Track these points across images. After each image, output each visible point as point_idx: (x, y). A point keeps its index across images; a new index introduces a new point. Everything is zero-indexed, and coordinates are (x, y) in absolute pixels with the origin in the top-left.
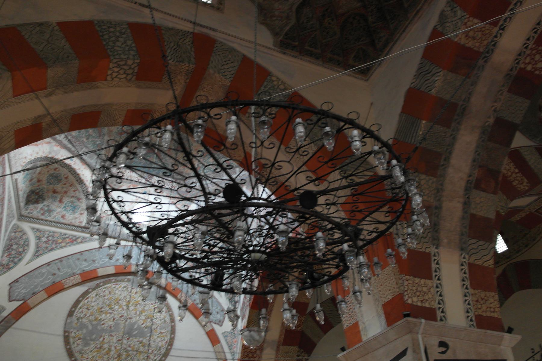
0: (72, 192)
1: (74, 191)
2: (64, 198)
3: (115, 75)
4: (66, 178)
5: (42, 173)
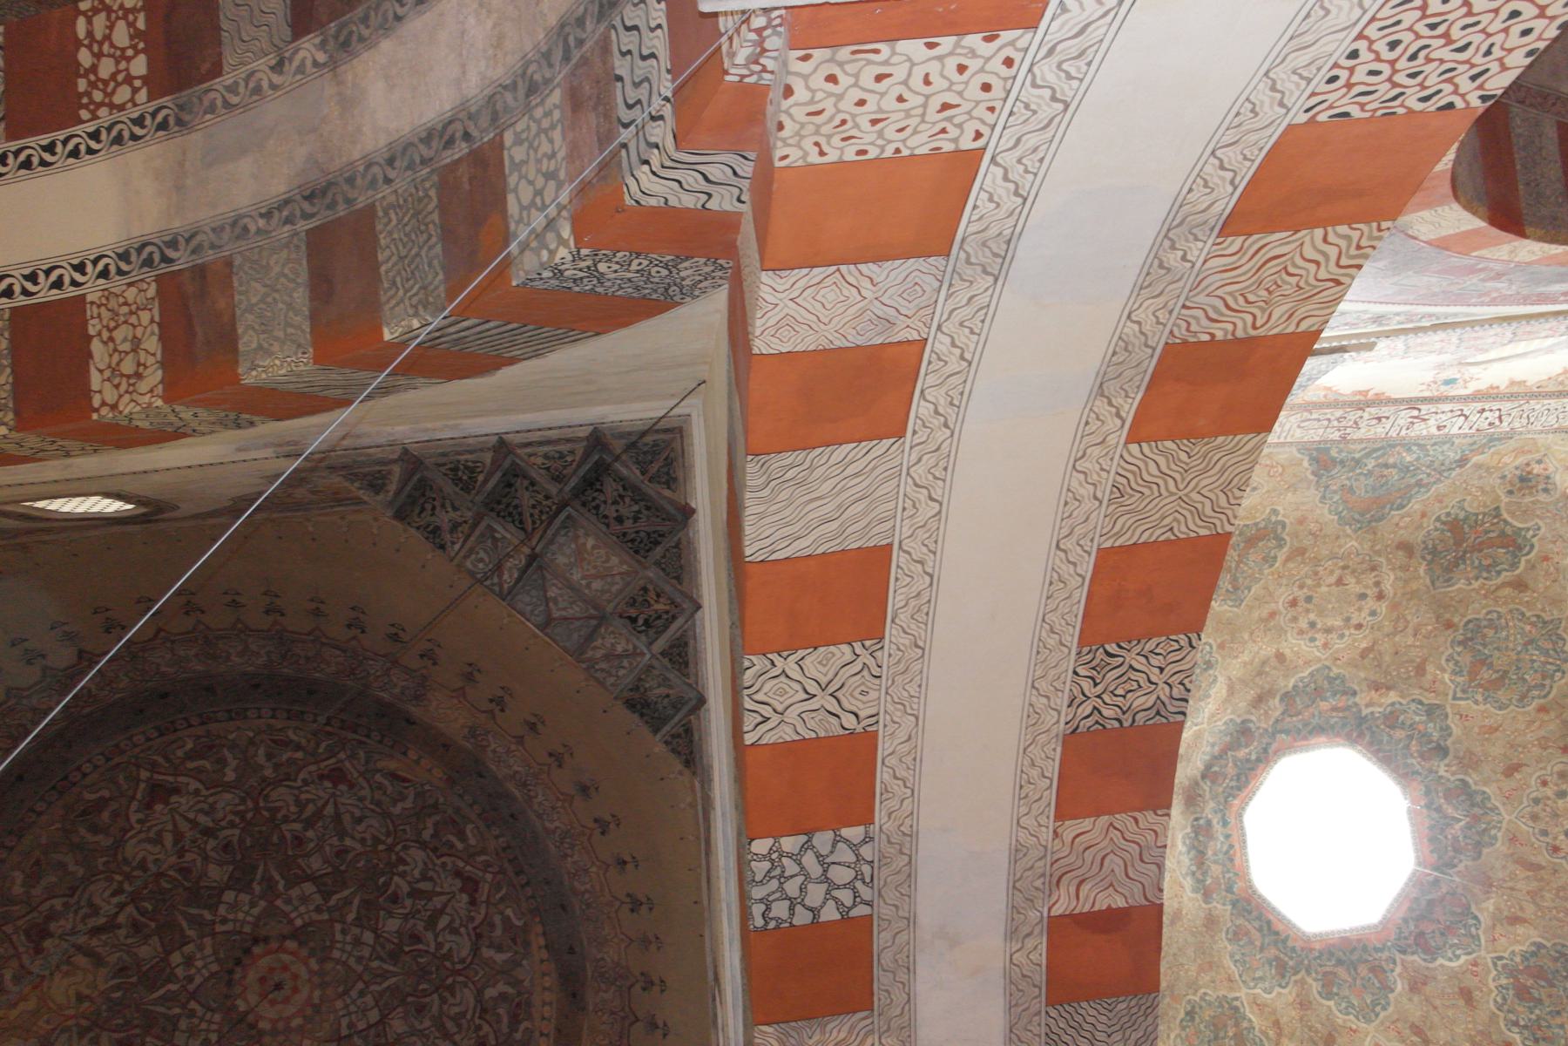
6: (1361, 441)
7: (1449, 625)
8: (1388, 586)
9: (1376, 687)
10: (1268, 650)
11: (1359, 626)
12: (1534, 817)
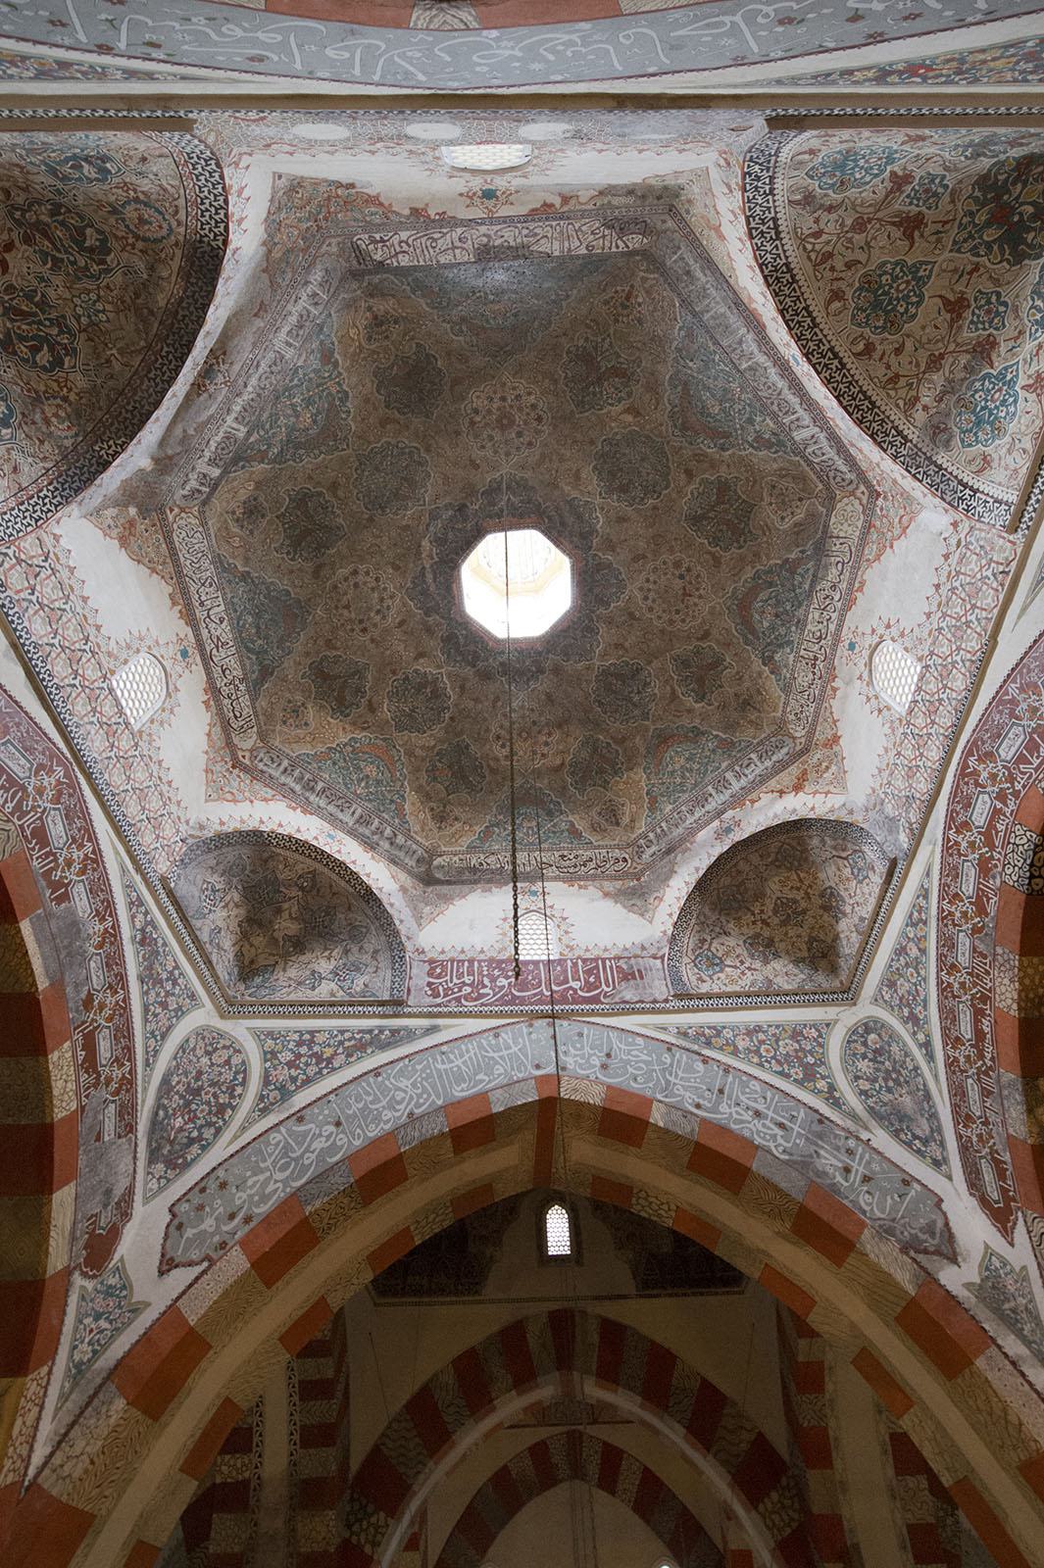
0: (831, 228)
1: (817, 234)
2: (881, 195)
3: (665, 1207)
4: (837, 295)
5: (923, 357)
6: (243, 667)
7: (371, 520)
8: (342, 572)
9: (418, 553)
10: (398, 634)
11: (377, 580)
12: (508, 454)
